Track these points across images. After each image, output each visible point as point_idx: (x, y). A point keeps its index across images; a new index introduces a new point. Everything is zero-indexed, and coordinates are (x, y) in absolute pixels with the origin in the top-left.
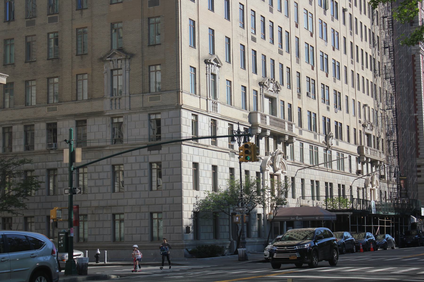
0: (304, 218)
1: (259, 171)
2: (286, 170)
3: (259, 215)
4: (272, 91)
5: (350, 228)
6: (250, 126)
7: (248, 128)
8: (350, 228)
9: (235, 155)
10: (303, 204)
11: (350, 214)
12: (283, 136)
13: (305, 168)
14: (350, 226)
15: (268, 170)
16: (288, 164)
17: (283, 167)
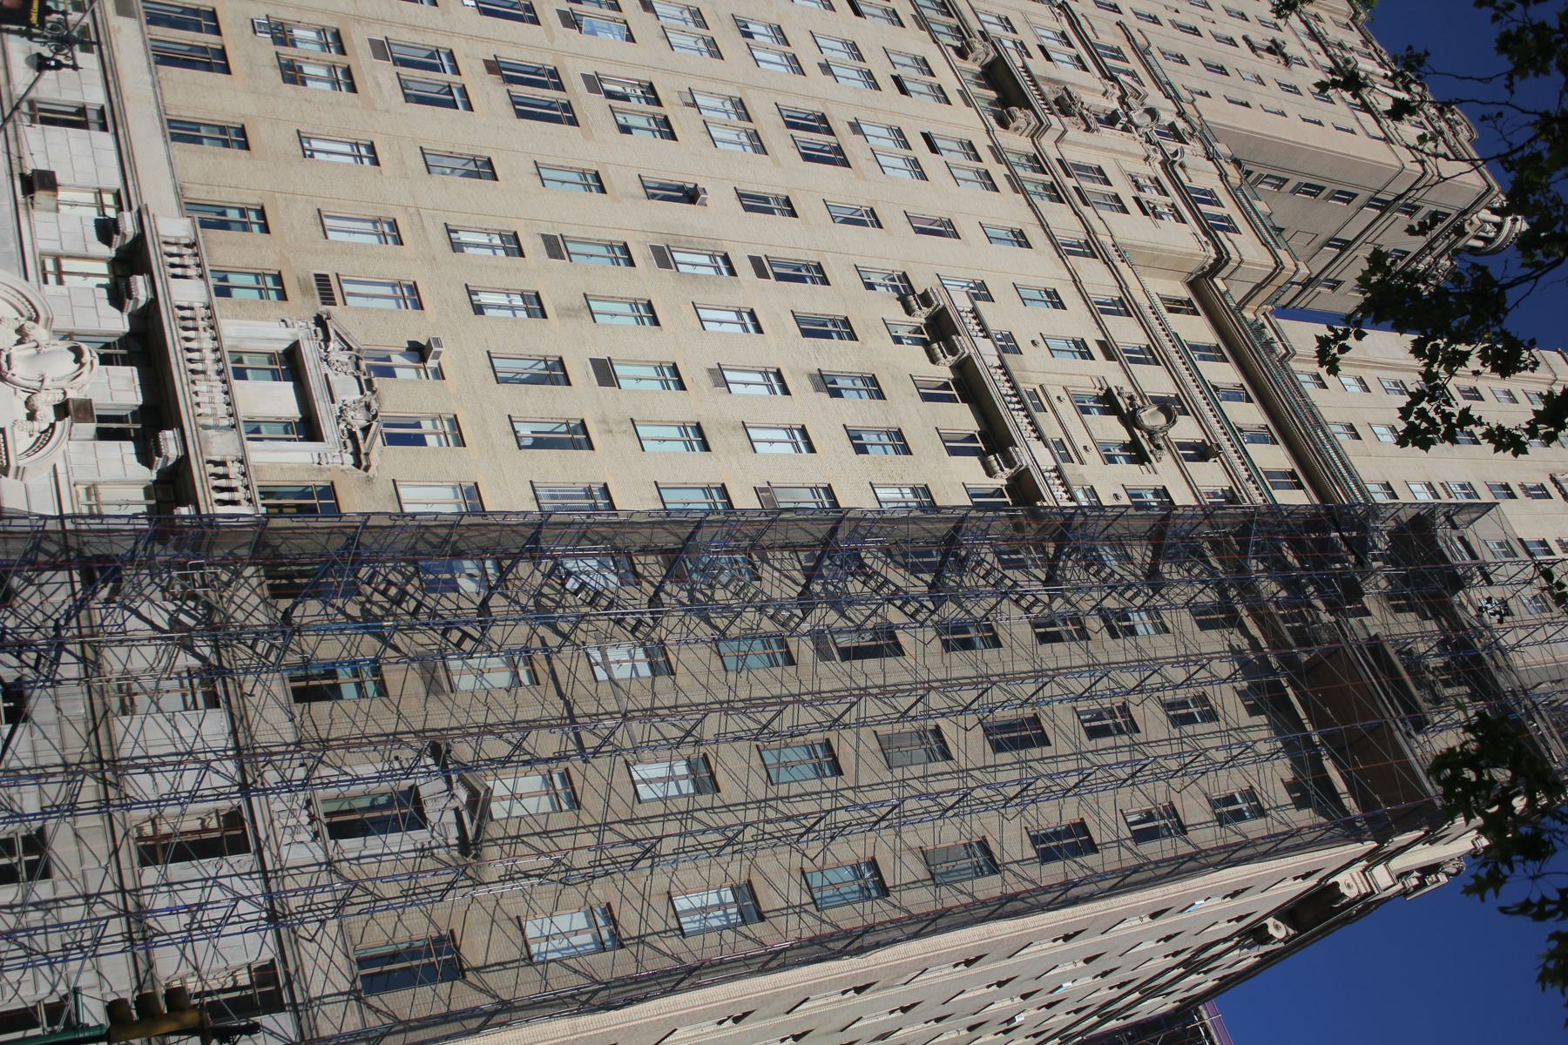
4: (333, 402)
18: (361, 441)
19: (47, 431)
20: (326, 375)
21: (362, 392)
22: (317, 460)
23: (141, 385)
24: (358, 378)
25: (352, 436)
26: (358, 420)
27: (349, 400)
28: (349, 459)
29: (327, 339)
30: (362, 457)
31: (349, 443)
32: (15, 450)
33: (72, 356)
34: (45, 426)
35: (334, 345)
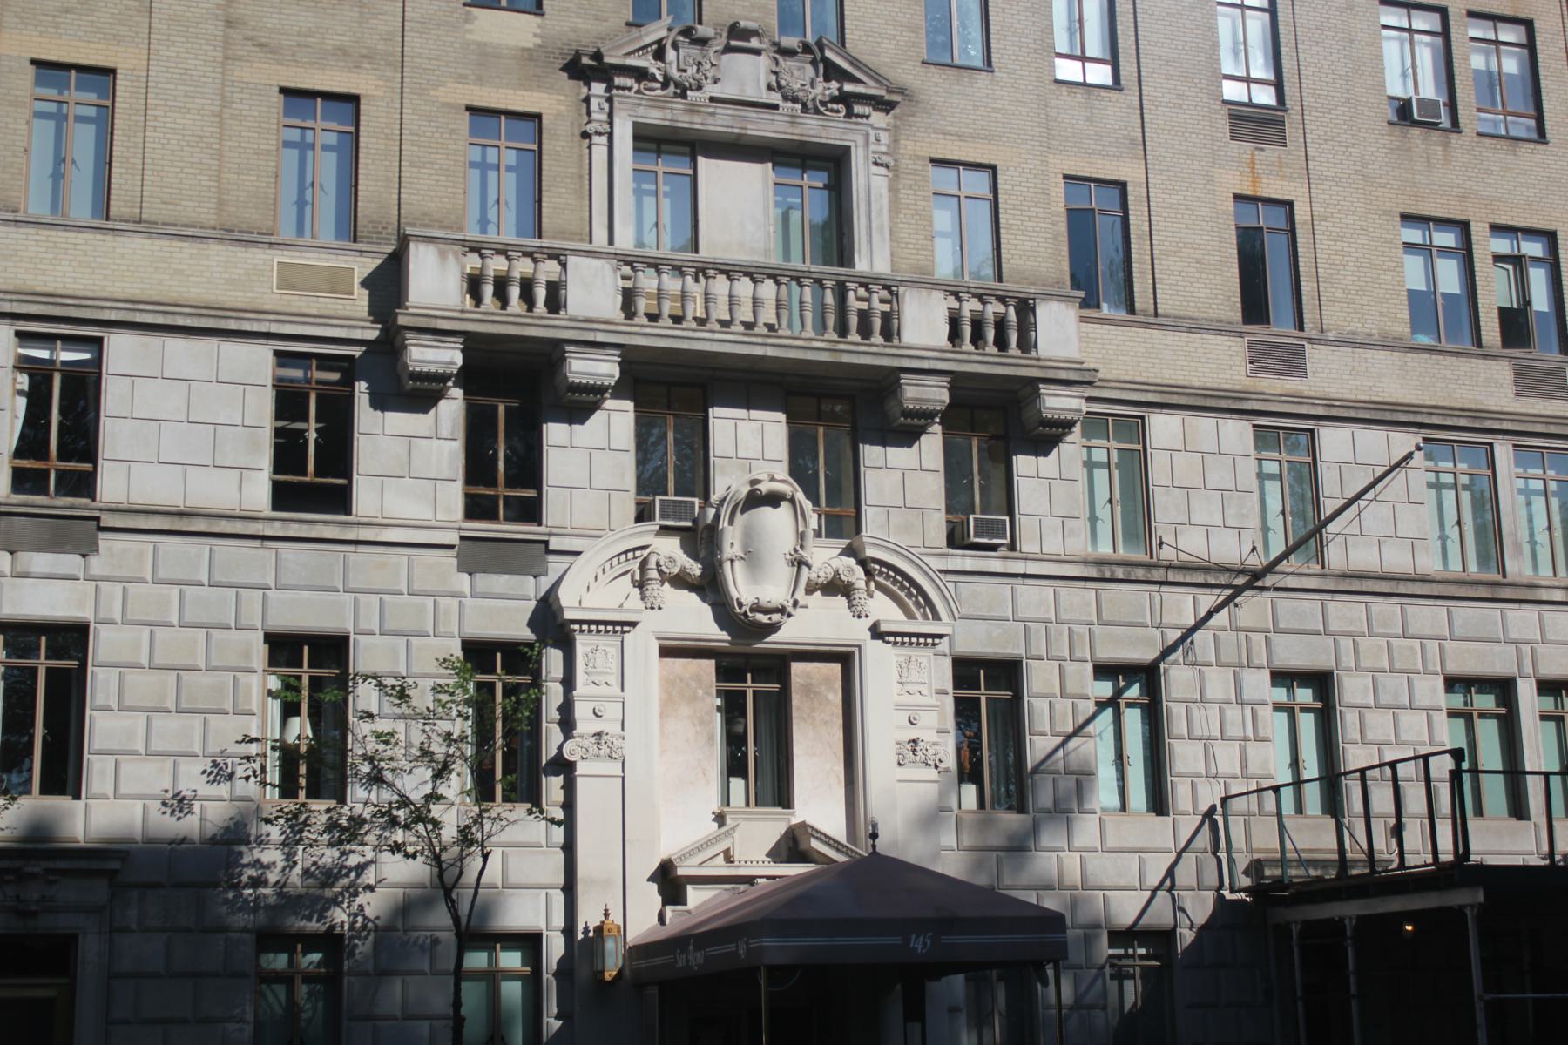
0: (713, 951)
1: (527, 634)
2: (936, 617)
3: (530, 942)
4: (775, 107)
5: (1480, 1018)
6: (372, 334)
7: (356, 352)
8: (1480, 1018)
9: (102, 535)
10: (1304, 851)
11: (1472, 906)
12: (883, 383)
13: (1239, 590)
14: (1479, 1006)
15: (633, 624)
16: (941, 571)
17: (910, 595)
18: (860, 89)
19: (868, 573)
20: (712, 99)
21: (757, 52)
22: (883, 170)
23: (748, 406)
24: (729, 49)
25: (845, 99)
26: (799, 74)
27: (764, 78)
28: (878, 118)
29: (641, 74)
30: (887, 97)
31: (857, 109)
32: (901, 622)
33: (767, 511)
34: (860, 571)
35: (646, 62)
